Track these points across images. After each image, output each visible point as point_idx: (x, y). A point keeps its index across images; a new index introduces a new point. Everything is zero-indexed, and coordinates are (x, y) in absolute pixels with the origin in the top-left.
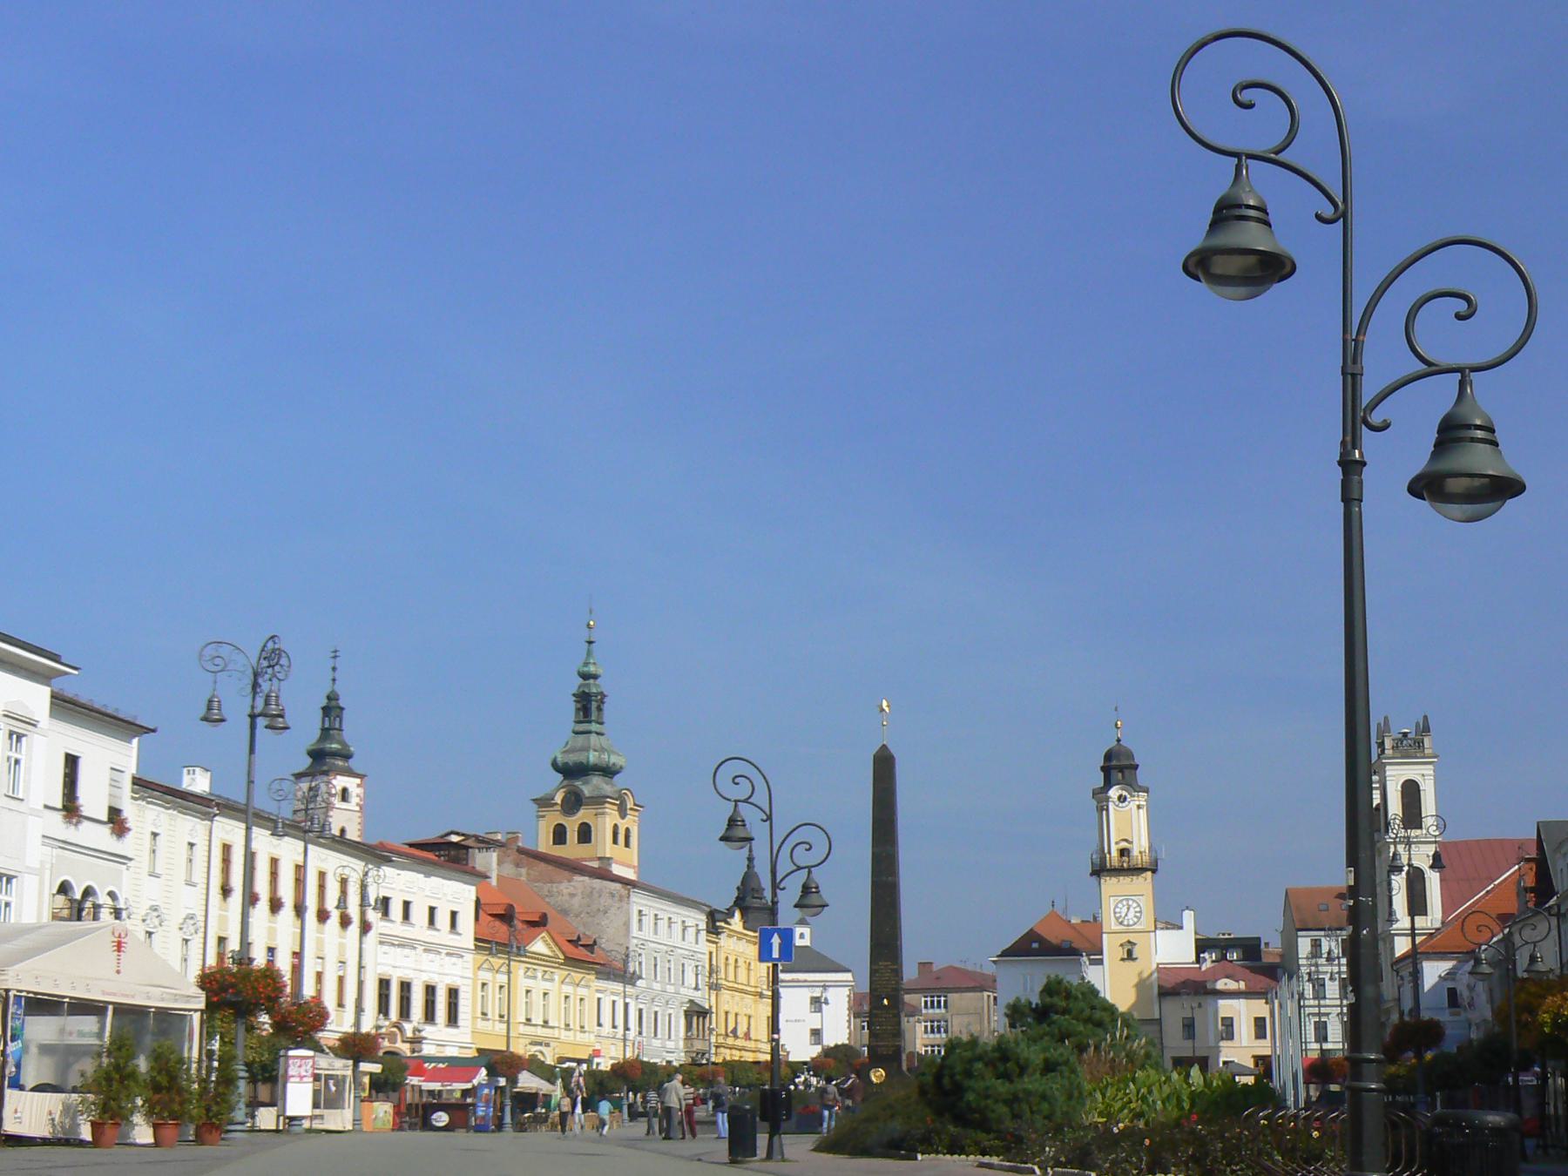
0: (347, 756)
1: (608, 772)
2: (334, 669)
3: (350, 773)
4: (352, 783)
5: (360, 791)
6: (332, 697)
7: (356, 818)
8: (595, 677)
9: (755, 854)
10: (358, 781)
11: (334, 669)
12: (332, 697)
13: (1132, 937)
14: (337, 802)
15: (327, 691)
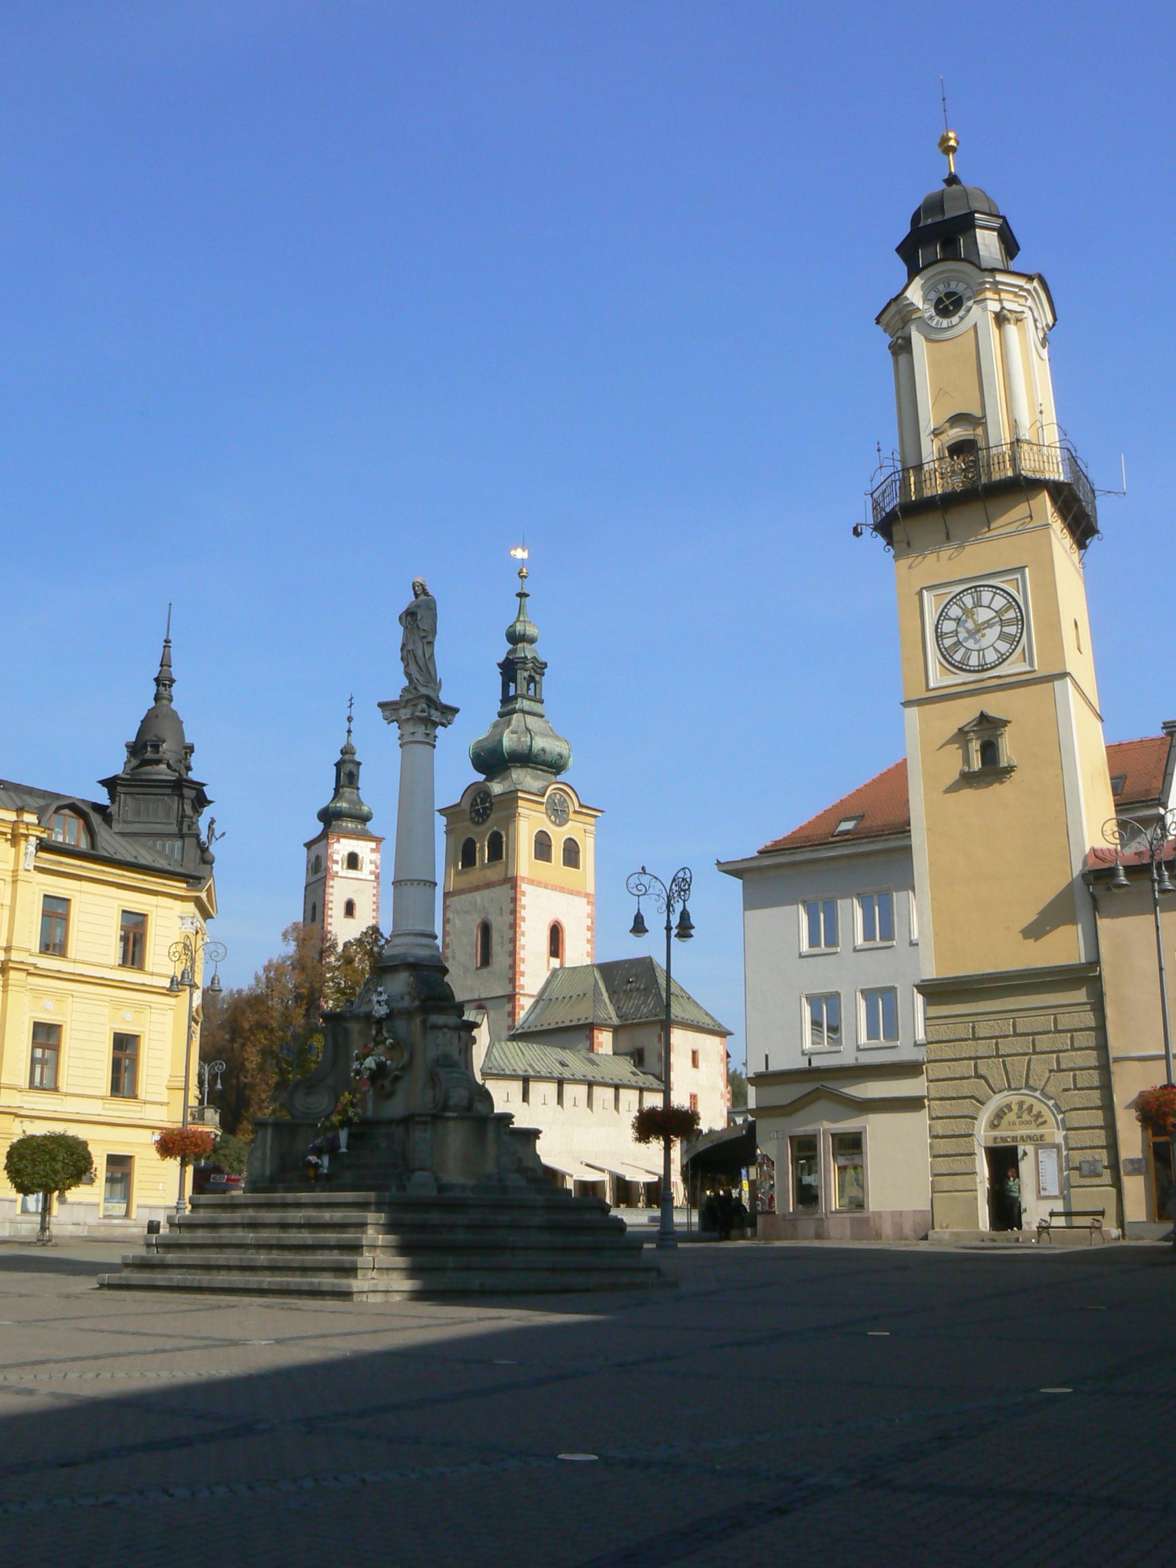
0: (365, 819)
1: (555, 766)
2: (350, 719)
3: (364, 836)
4: (363, 848)
5: (375, 857)
6: (347, 751)
7: (370, 889)
8: (532, 641)
9: (175, 672)
10: (373, 845)
11: (350, 719)
12: (347, 751)
13: (994, 705)
14: (339, 868)
15: (343, 744)
